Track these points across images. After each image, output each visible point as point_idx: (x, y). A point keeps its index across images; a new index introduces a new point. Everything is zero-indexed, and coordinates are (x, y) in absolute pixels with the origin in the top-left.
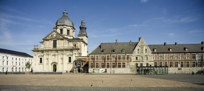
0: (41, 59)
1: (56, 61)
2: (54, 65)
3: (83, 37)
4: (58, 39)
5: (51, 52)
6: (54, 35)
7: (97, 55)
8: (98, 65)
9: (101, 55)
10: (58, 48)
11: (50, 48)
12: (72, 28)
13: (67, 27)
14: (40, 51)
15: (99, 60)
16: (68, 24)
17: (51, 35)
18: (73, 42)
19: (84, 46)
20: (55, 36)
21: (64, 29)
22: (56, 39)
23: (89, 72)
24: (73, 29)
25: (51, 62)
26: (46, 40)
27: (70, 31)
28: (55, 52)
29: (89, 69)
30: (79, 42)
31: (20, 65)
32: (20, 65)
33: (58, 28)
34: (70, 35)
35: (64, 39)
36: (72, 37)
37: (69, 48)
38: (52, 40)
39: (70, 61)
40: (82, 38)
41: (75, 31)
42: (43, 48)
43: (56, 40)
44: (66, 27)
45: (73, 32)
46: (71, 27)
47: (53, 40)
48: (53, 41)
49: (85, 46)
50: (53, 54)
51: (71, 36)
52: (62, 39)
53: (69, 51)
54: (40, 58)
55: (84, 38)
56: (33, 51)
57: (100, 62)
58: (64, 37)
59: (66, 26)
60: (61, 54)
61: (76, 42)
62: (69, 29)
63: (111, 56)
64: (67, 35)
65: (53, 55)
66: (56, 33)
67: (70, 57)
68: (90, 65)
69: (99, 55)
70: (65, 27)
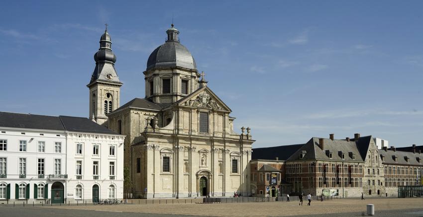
0: (166, 160)
1: (207, 169)
2: (202, 178)
3: (112, 88)
4: (213, 111)
5: (197, 142)
6: (204, 98)
11: (195, 131)
17: (198, 97)
25: (195, 168)
28: (204, 143)
37: (234, 137)
39: (235, 170)
40: (110, 92)
42: (172, 128)
43: (208, 114)
50: (199, 148)
52: (221, 112)
53: (234, 145)
57: (331, 175)
58: (225, 109)
60: (220, 149)
63: (343, 165)
66: (207, 95)
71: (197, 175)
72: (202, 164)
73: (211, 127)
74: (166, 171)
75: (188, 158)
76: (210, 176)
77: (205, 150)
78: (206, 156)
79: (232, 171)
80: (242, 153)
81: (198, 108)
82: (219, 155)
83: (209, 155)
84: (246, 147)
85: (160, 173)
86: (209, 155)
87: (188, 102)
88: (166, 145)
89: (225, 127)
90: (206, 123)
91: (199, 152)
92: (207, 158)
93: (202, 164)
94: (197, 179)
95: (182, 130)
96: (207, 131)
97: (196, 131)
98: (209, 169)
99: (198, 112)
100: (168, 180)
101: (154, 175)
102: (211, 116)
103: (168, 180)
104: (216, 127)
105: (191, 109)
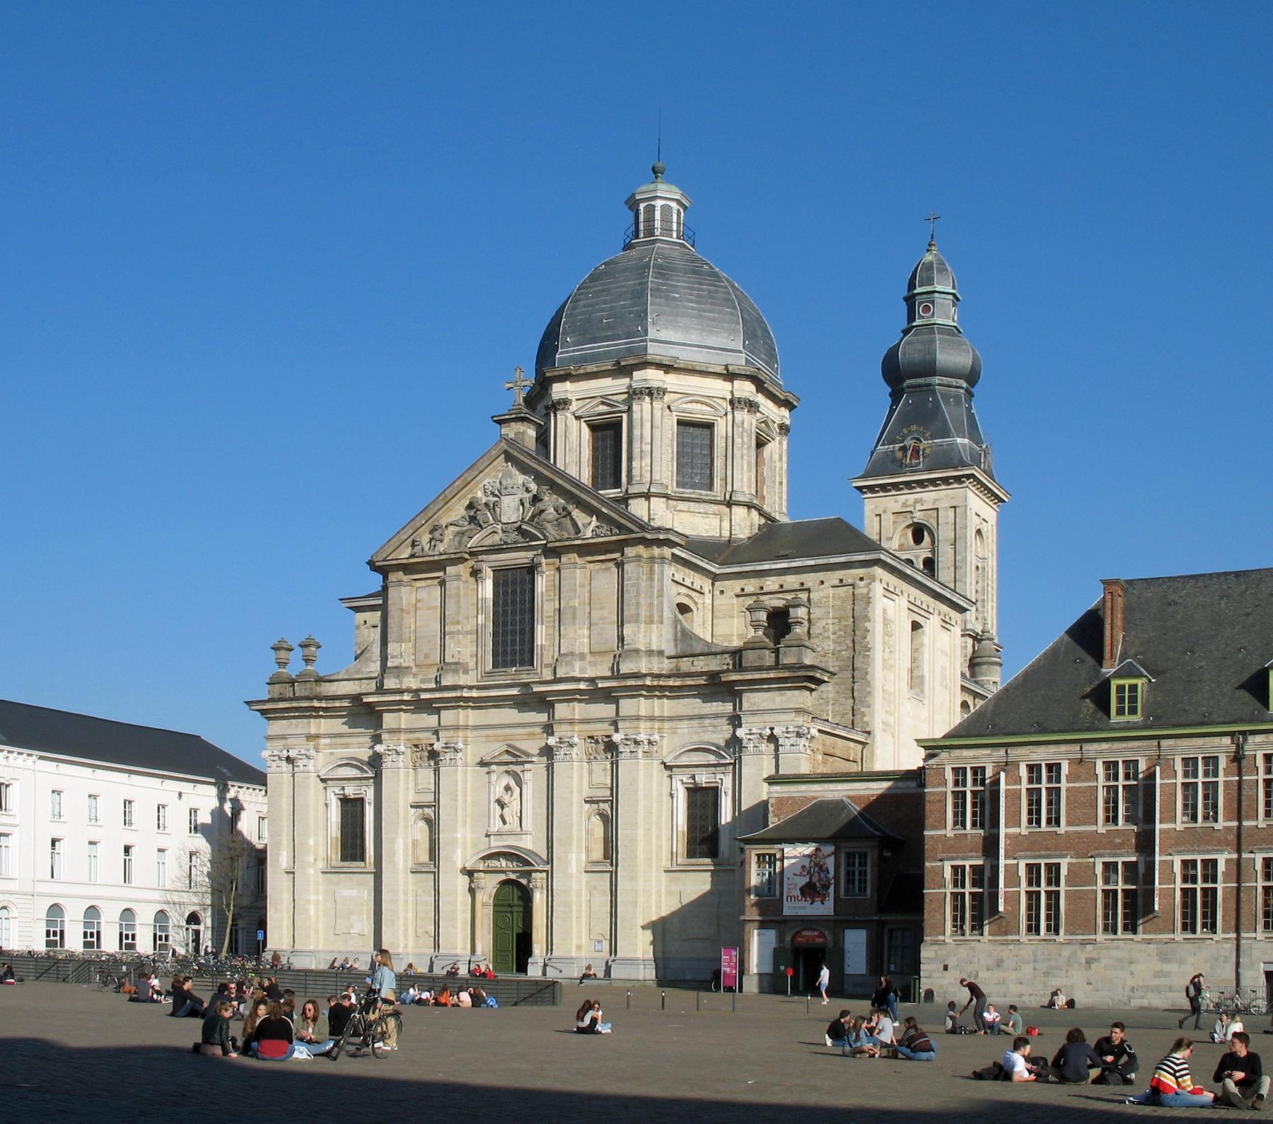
5: (471, 717)
7: (1042, 755)
8: (1054, 897)
9: (1100, 754)
10: (548, 675)
11: (458, 667)
12: (745, 389)
13: (671, 381)
14: (329, 713)
15: (1063, 828)
16: (686, 356)
18: (751, 586)
19: (916, 626)
20: (510, 510)
21: (642, 408)
22: (522, 557)
23: (925, 984)
24: (752, 406)
26: (407, 568)
27: (721, 429)
29: (926, 952)
30: (834, 577)
31: (127, 877)
32: (127, 877)
33: (565, 403)
34: (718, 491)
35: (620, 546)
36: (750, 506)
38: (475, 573)
41: (784, 429)
43: (532, 569)
44: (663, 391)
45: (760, 444)
46: (730, 376)
47: (490, 573)
48: (487, 588)
49: (932, 625)
51: (730, 504)
54: (345, 801)
55: (947, 516)
56: (263, 712)
57: (1084, 846)
58: (621, 527)
59: (668, 368)
61: (791, 581)
62: (700, 412)
64: (672, 489)
65: (483, 764)
66: (520, 478)
67: (703, 778)
68: (950, 889)
69: (1063, 755)
70: (650, 392)
71: (470, 873)
72: (504, 822)
73: (541, 634)
74: (354, 859)
75: (430, 798)
76: (539, 879)
77: (507, 752)
78: (519, 783)
79: (681, 847)
80: (741, 748)
81: (472, 554)
82: (590, 772)
83: (534, 776)
84: (753, 713)
85: (321, 865)
86: (534, 776)
87: (425, 538)
88: (347, 745)
89: (622, 625)
90: (527, 617)
91: (483, 764)
92: (528, 789)
93: (504, 822)
94: (472, 891)
95: (400, 671)
96: (527, 656)
97: (472, 665)
98: (531, 842)
99: (475, 573)
100: (357, 890)
101: (294, 873)
102: (541, 584)
103: (357, 890)
104: (579, 637)
105: (440, 565)
